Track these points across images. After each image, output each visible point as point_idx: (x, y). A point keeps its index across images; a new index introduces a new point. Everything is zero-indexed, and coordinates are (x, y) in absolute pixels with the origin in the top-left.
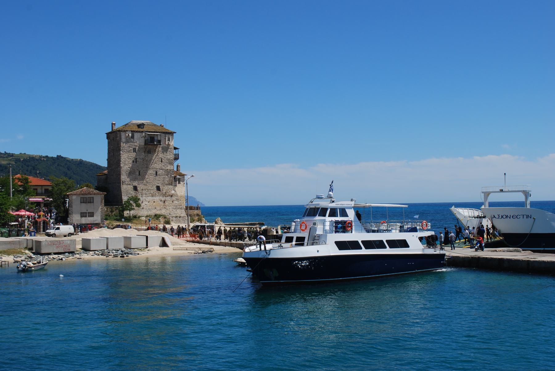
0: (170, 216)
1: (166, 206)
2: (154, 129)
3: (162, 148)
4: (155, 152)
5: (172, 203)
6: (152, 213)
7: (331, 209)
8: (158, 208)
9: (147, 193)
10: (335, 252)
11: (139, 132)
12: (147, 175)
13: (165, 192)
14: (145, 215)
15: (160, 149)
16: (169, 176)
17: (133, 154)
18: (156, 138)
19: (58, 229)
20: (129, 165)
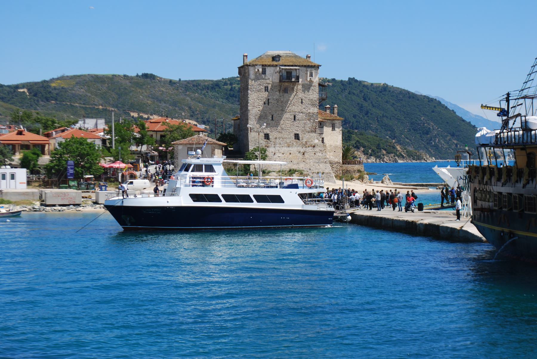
0: (310, 171)
1: (305, 159)
2: (292, 62)
3: (303, 85)
4: (293, 91)
6: (287, 168)
7: (194, 165)
8: (295, 162)
10: (190, 203)
11: (273, 66)
12: (282, 120)
13: (305, 141)
14: (278, 170)
15: (300, 87)
17: (264, 93)
18: (294, 74)
19: (132, 183)
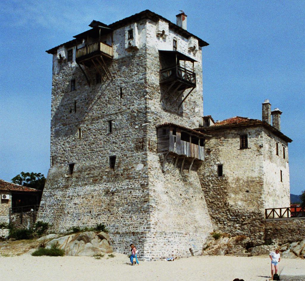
9: (87, 176)
13: (122, 168)
16: (137, 127)
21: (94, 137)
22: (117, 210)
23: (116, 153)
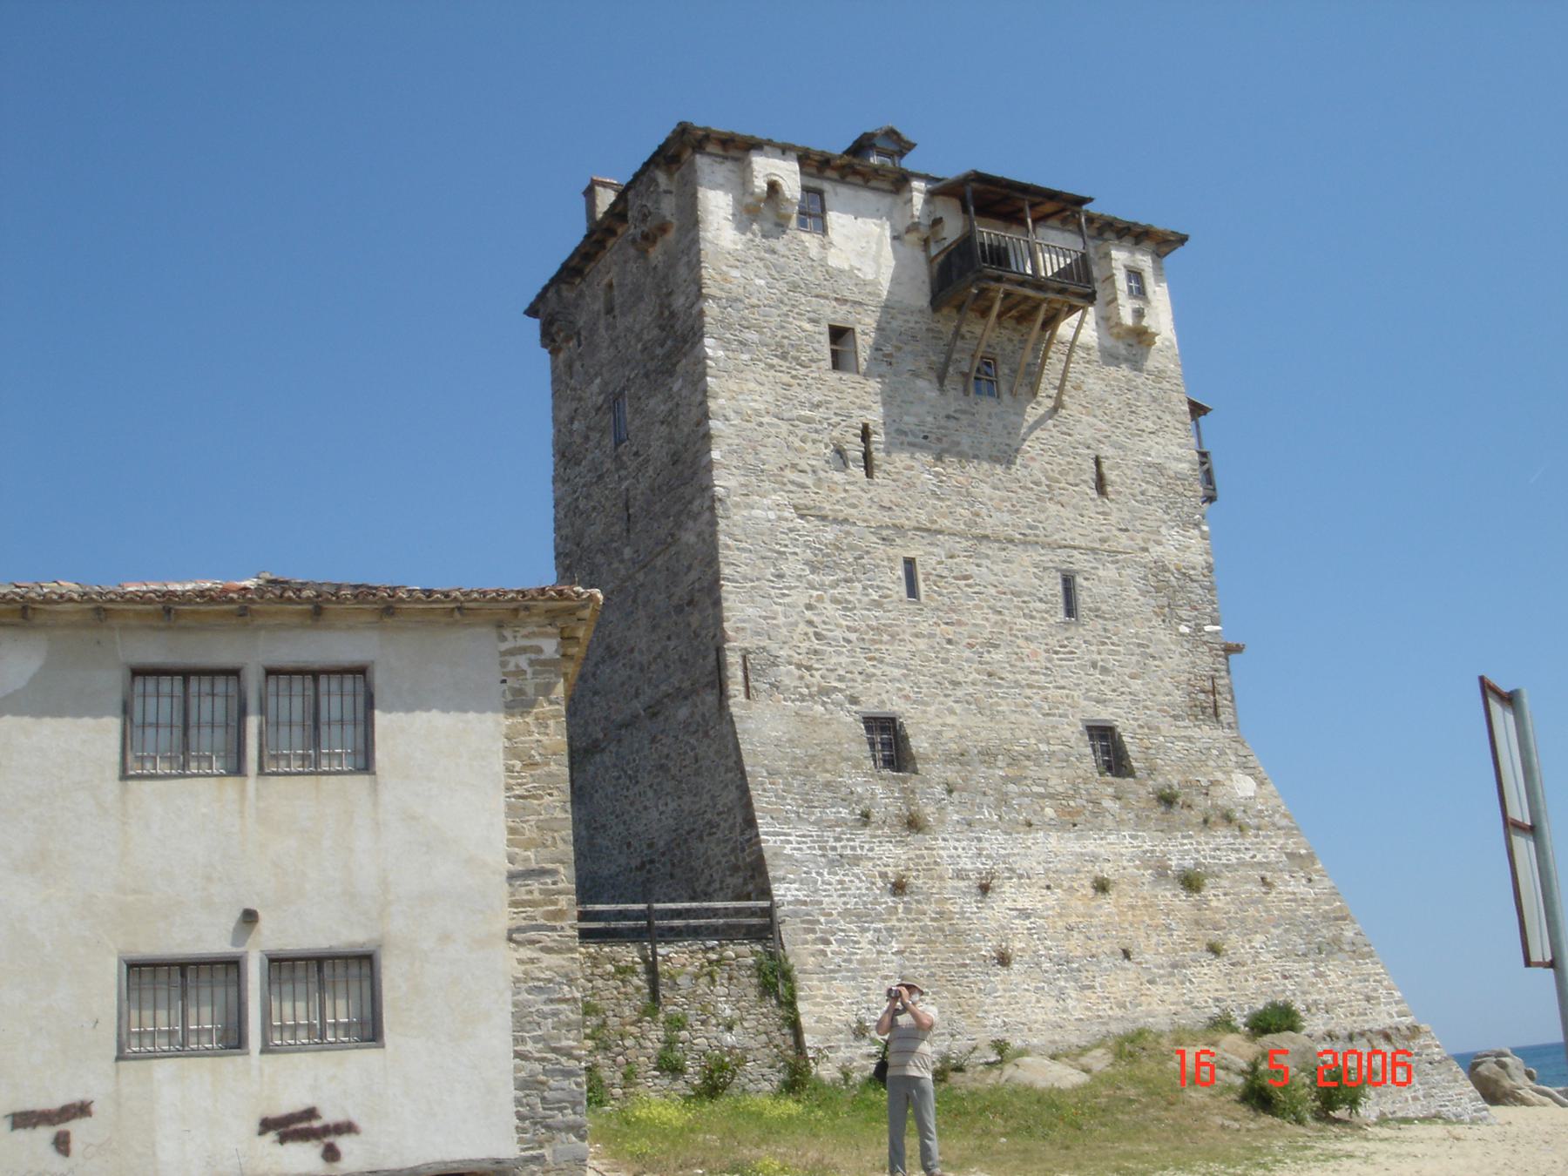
4: (1034, 391)
5: (1258, 890)
8: (1151, 953)
9: (1012, 787)
16: (1184, 629)
20: (802, 486)
21: (994, 617)
22: (1247, 946)
23: (1111, 710)
